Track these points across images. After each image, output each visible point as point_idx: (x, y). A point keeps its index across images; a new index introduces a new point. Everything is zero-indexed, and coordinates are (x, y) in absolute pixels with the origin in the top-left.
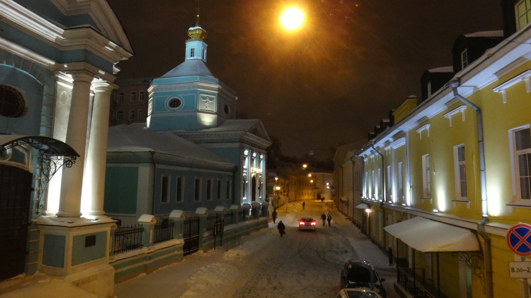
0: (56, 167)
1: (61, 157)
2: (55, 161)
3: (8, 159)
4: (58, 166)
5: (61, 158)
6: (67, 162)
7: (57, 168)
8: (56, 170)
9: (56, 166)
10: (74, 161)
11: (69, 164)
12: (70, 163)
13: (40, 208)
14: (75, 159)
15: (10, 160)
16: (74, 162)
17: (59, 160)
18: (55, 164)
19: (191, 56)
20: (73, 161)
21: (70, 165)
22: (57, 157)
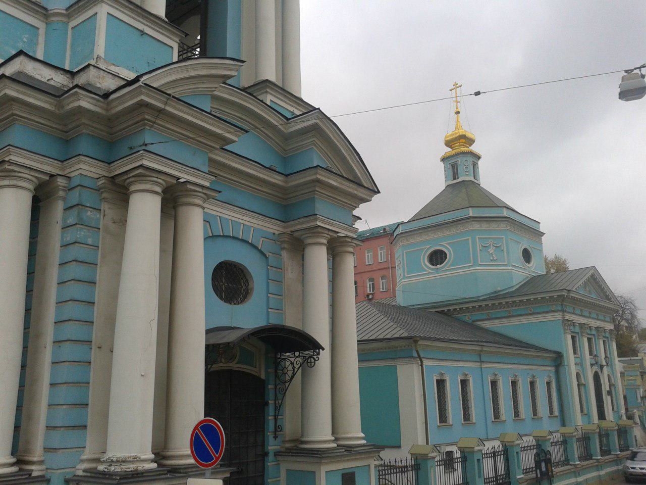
0: (294, 368)
1: (300, 353)
2: (292, 360)
3: (236, 360)
4: (297, 366)
5: (299, 355)
6: (308, 359)
7: (296, 370)
8: (295, 371)
9: (294, 367)
10: (317, 357)
11: (311, 362)
12: (313, 360)
13: (279, 430)
14: (318, 354)
15: (237, 363)
16: (317, 359)
17: (297, 357)
18: (292, 363)
19: (454, 179)
20: (315, 357)
21: (313, 364)
22: (294, 354)
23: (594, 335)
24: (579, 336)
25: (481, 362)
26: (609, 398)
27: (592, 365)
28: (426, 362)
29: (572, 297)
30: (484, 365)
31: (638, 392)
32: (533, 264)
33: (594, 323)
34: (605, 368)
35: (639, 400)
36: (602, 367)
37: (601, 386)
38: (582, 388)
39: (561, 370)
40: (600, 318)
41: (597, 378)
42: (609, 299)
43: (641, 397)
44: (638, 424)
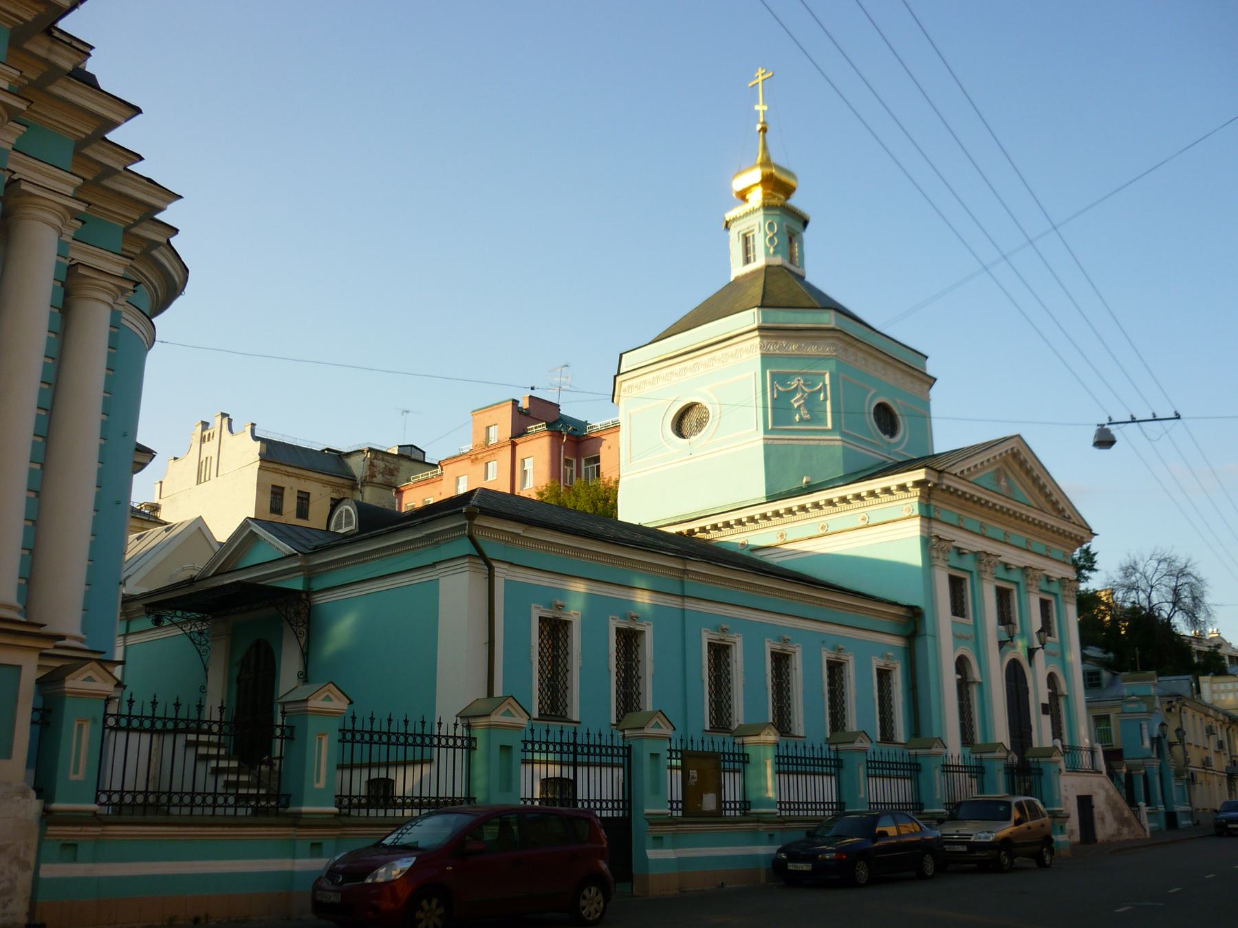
23: (1017, 583)
24: (972, 578)
25: (683, 596)
26: (1046, 720)
27: (1002, 644)
28: (501, 572)
29: (949, 487)
30: (690, 605)
31: (1145, 726)
32: (905, 432)
33: (1015, 558)
34: (1040, 655)
35: (1147, 743)
36: (1031, 652)
37: (1028, 693)
38: (974, 692)
39: (919, 643)
40: (1052, 555)
41: (1015, 676)
42: (1061, 512)
43: (1152, 739)
44: (1101, 772)
